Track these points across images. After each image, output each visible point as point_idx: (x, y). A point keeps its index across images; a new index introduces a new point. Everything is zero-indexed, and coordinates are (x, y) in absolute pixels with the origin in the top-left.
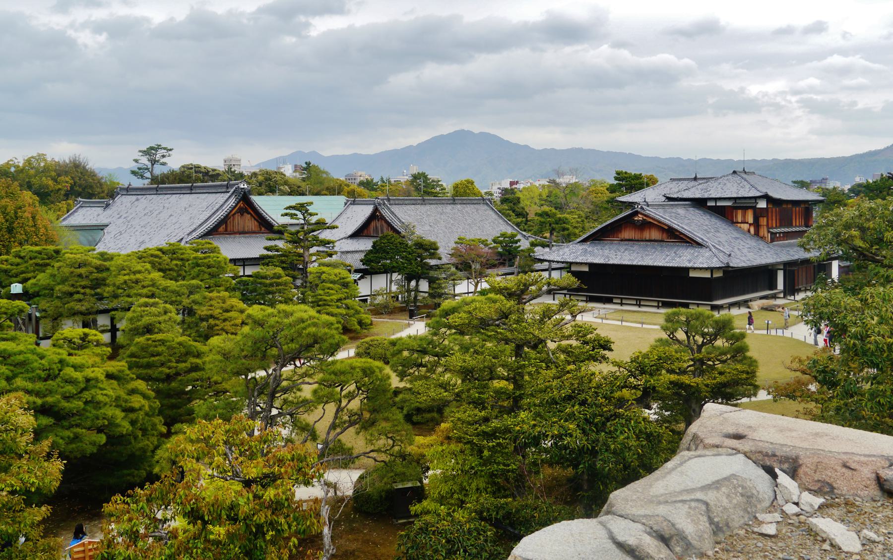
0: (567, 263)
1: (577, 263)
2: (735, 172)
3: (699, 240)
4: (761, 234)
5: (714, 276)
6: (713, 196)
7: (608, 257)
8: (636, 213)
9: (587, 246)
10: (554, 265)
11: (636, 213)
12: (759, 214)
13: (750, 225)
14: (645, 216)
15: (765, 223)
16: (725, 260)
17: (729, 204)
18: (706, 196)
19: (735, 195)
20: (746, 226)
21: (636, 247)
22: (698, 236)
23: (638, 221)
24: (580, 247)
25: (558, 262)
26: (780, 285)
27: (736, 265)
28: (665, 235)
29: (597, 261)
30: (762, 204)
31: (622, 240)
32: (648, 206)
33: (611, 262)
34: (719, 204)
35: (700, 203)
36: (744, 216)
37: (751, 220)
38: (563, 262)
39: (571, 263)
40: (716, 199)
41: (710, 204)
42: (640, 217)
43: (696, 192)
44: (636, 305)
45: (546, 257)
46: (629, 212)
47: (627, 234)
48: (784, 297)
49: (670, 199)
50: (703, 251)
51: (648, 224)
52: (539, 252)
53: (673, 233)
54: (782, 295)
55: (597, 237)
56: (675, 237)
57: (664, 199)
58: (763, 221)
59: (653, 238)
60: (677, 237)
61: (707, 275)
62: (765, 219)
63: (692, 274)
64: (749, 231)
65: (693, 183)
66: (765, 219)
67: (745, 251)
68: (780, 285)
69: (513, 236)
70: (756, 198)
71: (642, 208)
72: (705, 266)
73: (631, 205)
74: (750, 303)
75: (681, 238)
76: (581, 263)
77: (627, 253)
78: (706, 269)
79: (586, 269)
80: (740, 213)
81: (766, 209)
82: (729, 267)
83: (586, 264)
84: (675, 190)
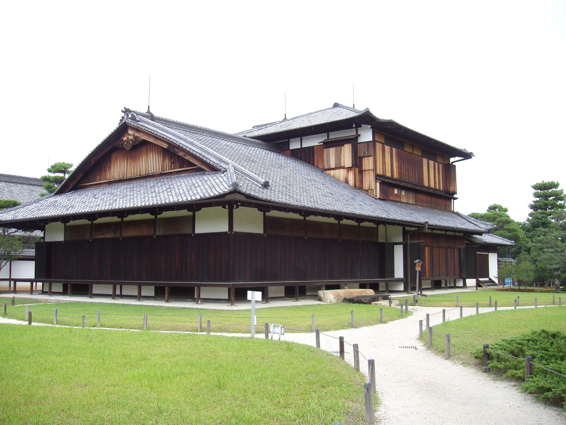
2: (336, 105)
3: (213, 160)
4: (366, 186)
13: (349, 169)
15: (371, 167)
20: (341, 174)
21: (122, 188)
23: (128, 141)
26: (399, 273)
28: (167, 163)
31: (110, 183)
36: (338, 157)
37: (347, 160)
41: (295, 145)
44: (114, 296)
48: (406, 290)
54: (401, 287)
58: (368, 163)
59: (151, 171)
62: (371, 159)
63: (201, 229)
64: (347, 182)
66: (371, 159)
68: (399, 273)
74: (321, 293)
79: (60, 238)
80: (332, 151)
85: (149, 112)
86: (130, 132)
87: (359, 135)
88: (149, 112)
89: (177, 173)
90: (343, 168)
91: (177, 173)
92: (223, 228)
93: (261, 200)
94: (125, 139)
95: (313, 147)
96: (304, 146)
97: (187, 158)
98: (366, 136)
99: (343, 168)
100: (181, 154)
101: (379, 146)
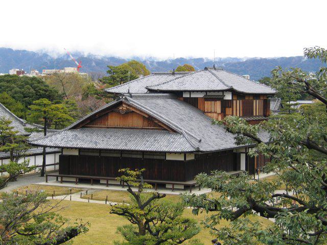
0: (59, 147)
1: (68, 148)
5: (187, 159)
6: (189, 89)
7: (96, 143)
8: (121, 103)
9: (78, 133)
10: (48, 150)
11: (121, 103)
12: (226, 105)
13: (219, 114)
14: (129, 106)
16: (197, 145)
17: (201, 96)
18: (182, 88)
19: (206, 89)
21: (120, 133)
22: (174, 122)
23: (122, 110)
24: (70, 134)
25: (51, 147)
27: (204, 150)
28: (146, 123)
29: (85, 146)
30: (228, 97)
31: (108, 128)
32: (131, 97)
33: (99, 147)
34: (193, 96)
35: (176, 95)
37: (219, 111)
38: (55, 147)
39: (63, 148)
40: (190, 92)
41: (186, 95)
42: (124, 107)
43: (174, 86)
45: (40, 142)
46: (115, 102)
47: (113, 120)
49: (151, 91)
50: (177, 137)
51: (132, 112)
52: (35, 138)
53: (153, 121)
55: (86, 124)
56: (154, 125)
57: (146, 91)
59: (135, 125)
60: (156, 125)
61: (181, 158)
63: (169, 158)
65: (172, 77)
67: (213, 137)
69: (8, 123)
70: (223, 91)
71: (126, 99)
72: (179, 150)
73: (116, 95)
75: (160, 126)
76: (72, 148)
77: (112, 139)
78: (180, 153)
79: (76, 153)
81: (233, 100)
82: (198, 151)
83: (76, 148)
84: (154, 81)
85: (129, 93)
86: (124, 105)
87: (225, 96)
88: (129, 93)
89: (152, 129)
90: (216, 113)
91: (152, 129)
92: (182, 159)
93: (204, 152)
94: (121, 108)
95: (197, 98)
96: (191, 96)
97: (160, 124)
98: (228, 97)
99: (216, 113)
100: (156, 122)
101: (234, 102)
